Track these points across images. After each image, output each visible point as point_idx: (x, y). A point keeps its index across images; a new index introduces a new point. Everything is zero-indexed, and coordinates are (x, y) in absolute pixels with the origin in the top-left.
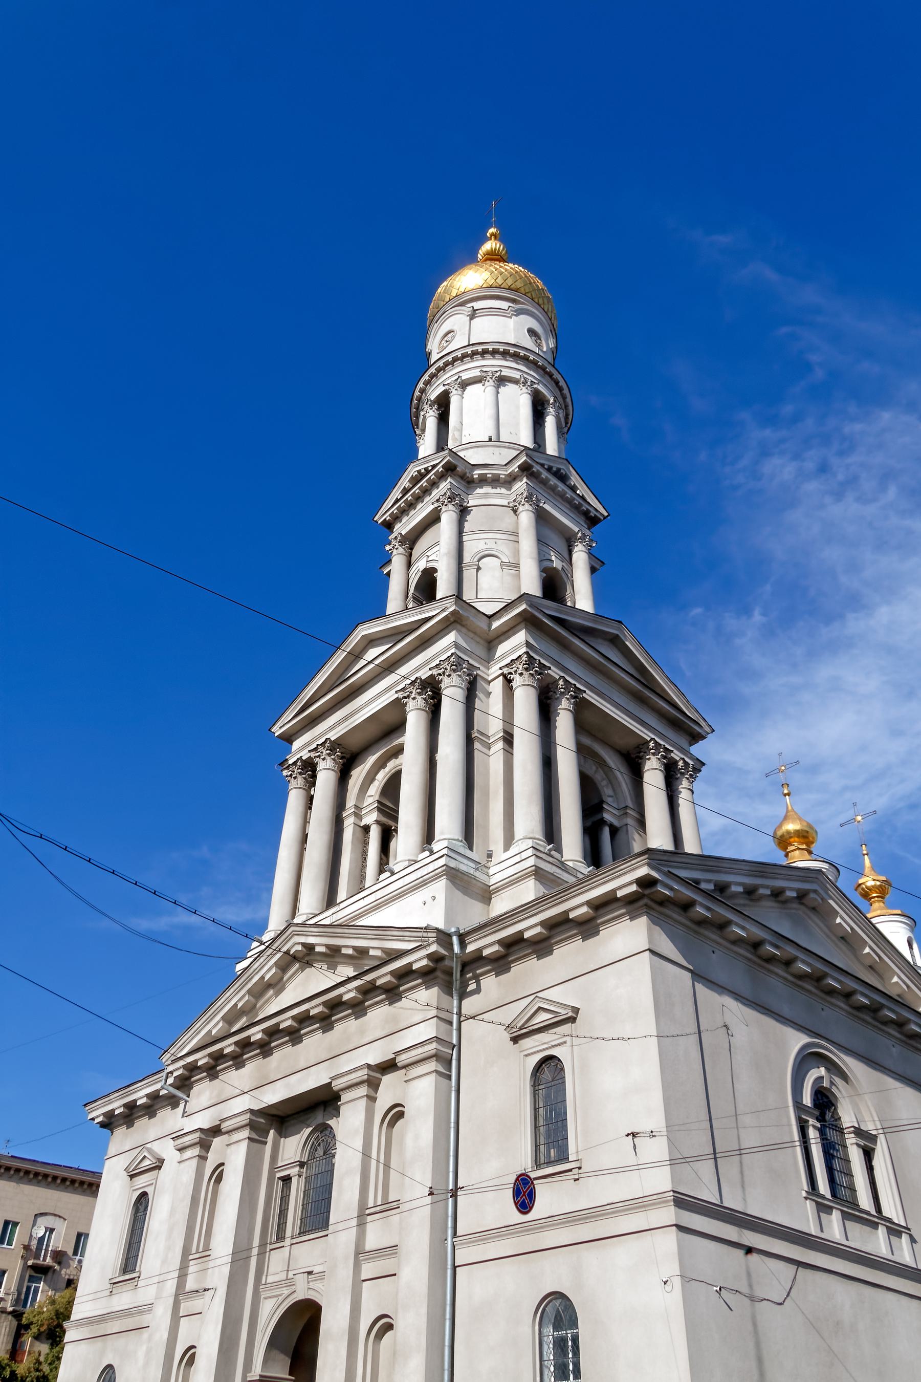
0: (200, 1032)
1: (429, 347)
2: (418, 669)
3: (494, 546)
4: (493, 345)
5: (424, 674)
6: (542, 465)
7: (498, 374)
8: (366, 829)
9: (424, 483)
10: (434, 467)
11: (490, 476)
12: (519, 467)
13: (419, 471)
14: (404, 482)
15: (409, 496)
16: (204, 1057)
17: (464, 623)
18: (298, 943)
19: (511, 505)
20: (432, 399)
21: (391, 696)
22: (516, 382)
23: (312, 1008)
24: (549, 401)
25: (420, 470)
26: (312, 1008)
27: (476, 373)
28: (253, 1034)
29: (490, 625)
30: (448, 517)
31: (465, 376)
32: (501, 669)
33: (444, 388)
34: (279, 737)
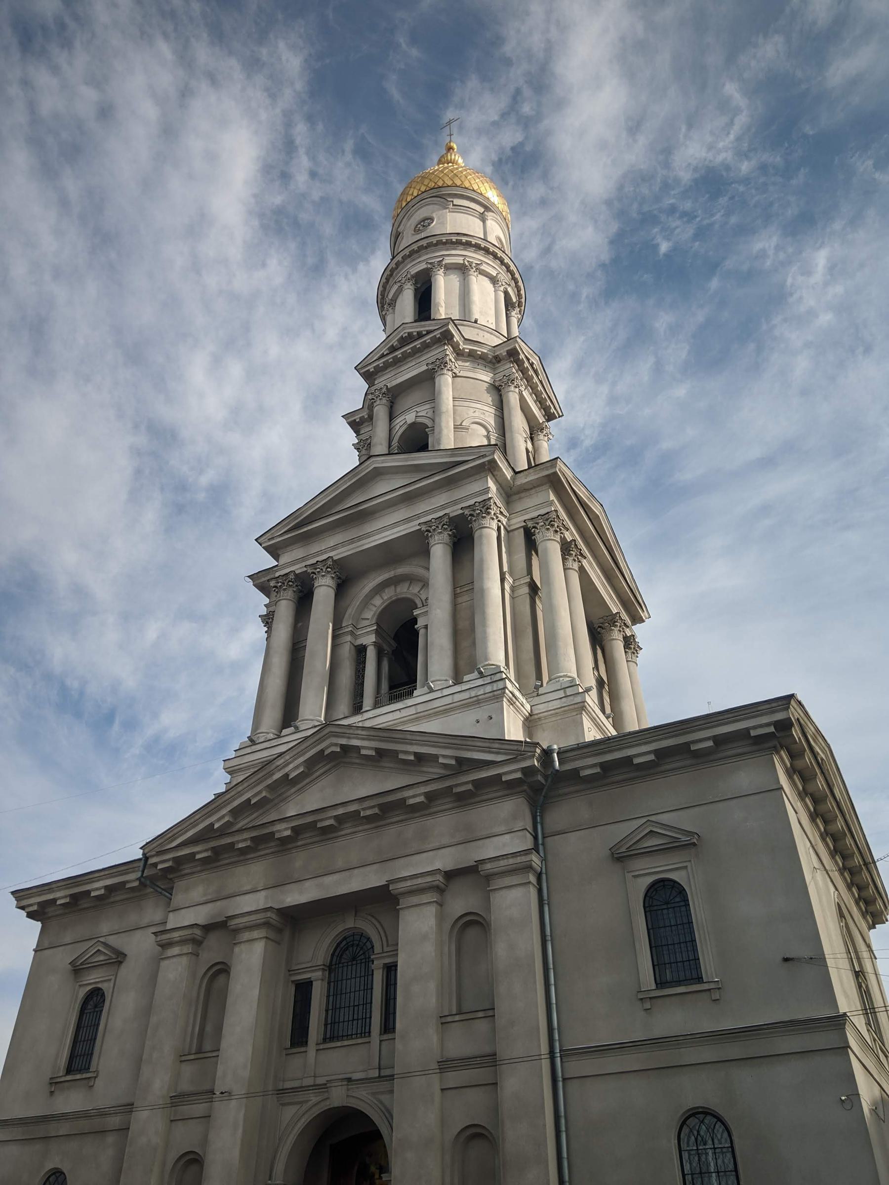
0: (197, 825)
3: (482, 416)
4: (476, 240)
8: (361, 651)
9: (417, 344)
10: (429, 332)
11: (480, 353)
12: (507, 351)
15: (400, 354)
16: (206, 850)
17: (495, 473)
18: (336, 745)
19: (497, 384)
20: (412, 273)
23: (364, 809)
25: (412, 332)
26: (364, 809)
28: (279, 831)
32: (525, 521)
33: (425, 266)
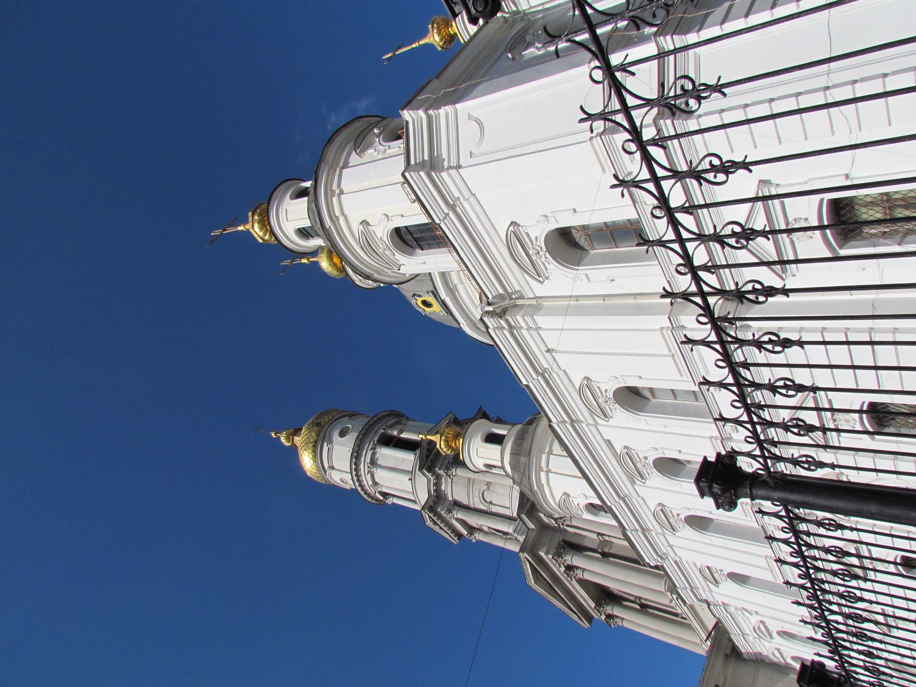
1: (349, 488)
2: (560, 572)
5: (563, 569)
6: (427, 457)
7: (369, 465)
10: (429, 516)
12: (429, 472)
13: (430, 521)
14: (436, 528)
21: (574, 582)
22: (374, 454)
24: (383, 433)
27: (369, 476)
29: (533, 529)
30: (460, 515)
31: (370, 483)
34: (590, 624)
